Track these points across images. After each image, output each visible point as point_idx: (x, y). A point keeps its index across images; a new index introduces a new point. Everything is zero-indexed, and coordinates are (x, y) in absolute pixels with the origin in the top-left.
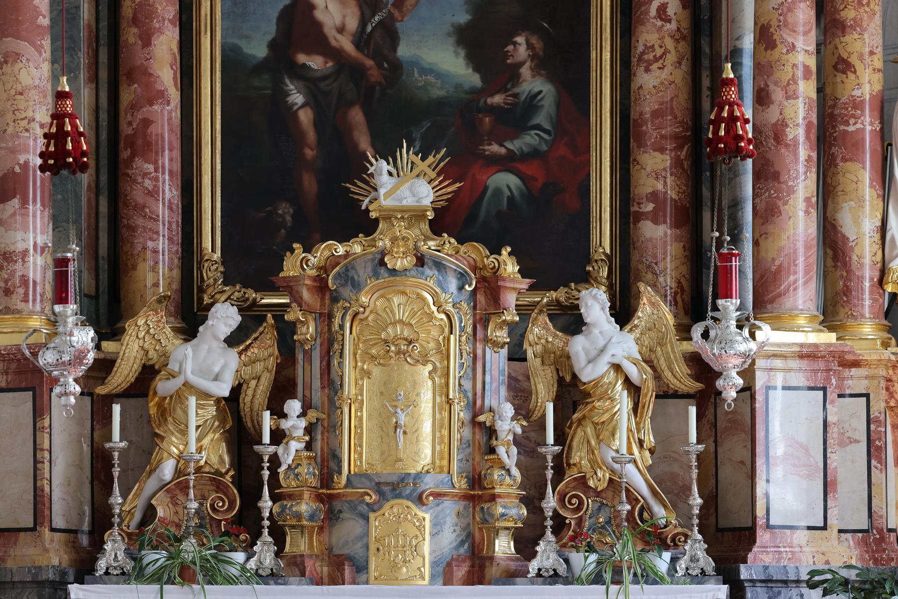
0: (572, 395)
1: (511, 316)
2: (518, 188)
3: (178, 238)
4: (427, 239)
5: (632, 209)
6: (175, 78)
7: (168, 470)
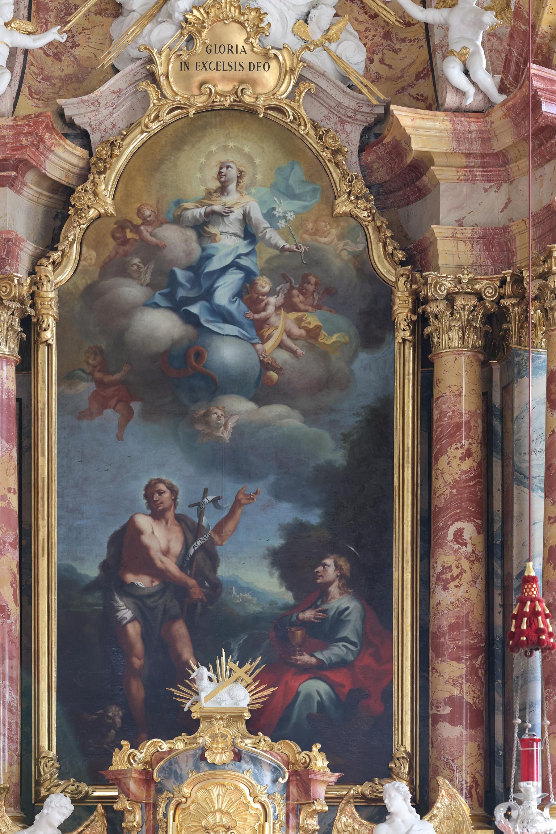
1: (321, 806)
2: (327, 693)
3: (18, 737)
4: (243, 737)
5: (431, 712)
6: (14, 595)
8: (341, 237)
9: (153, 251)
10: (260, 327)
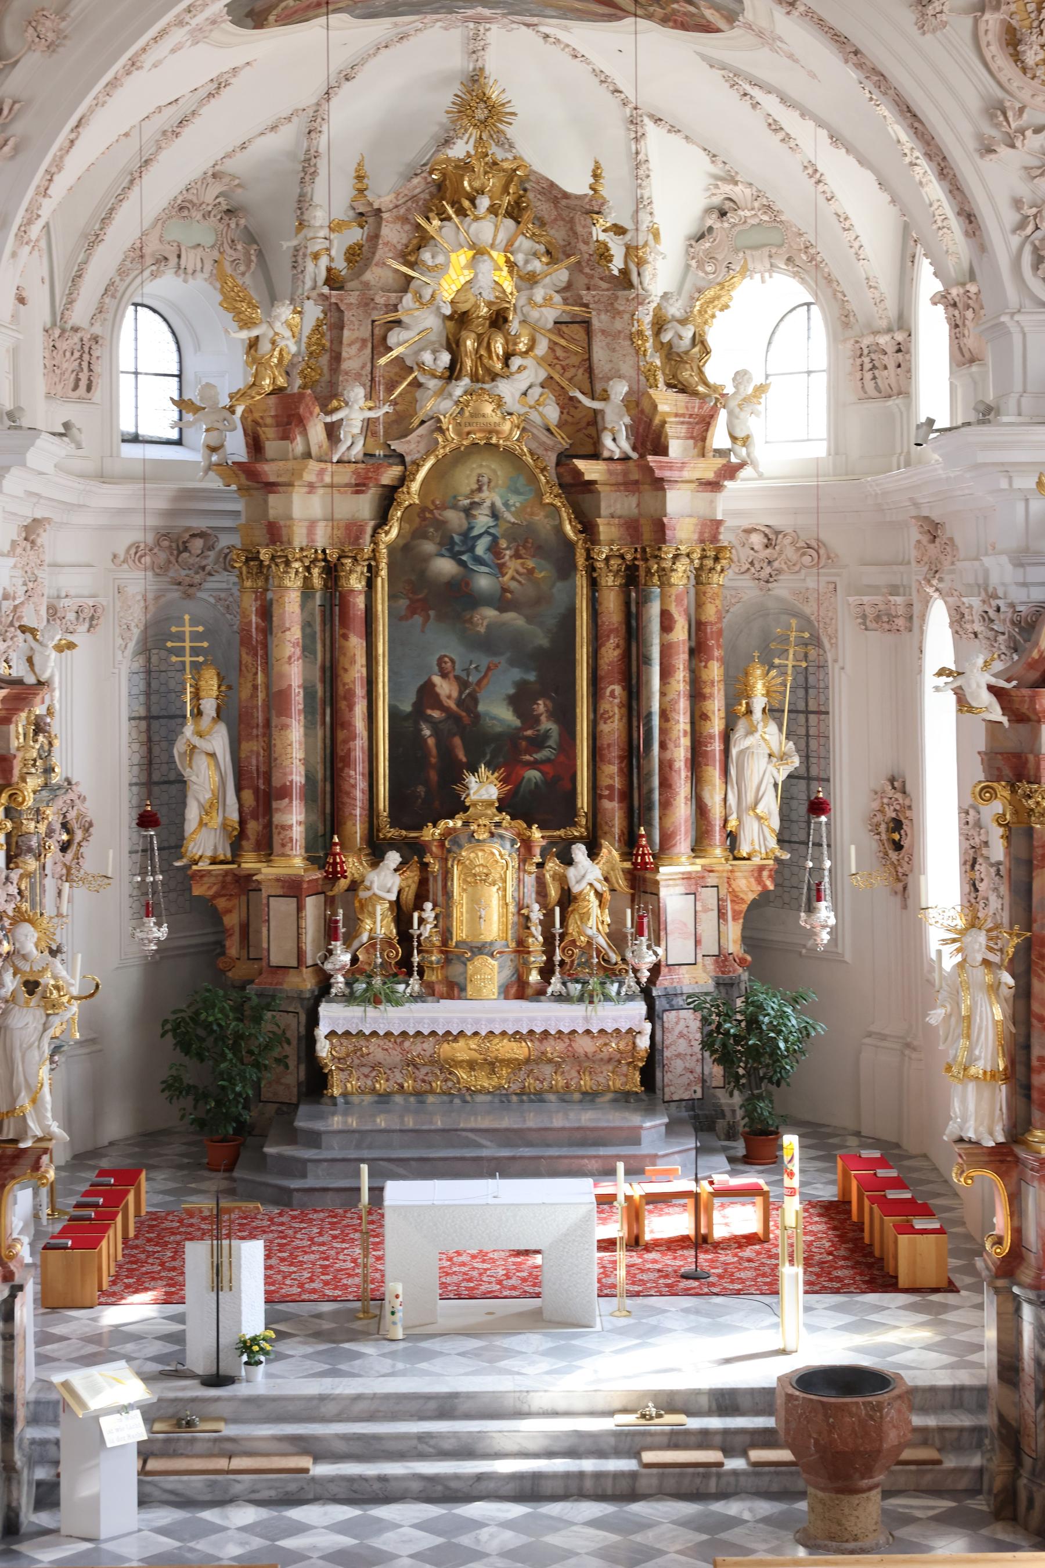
0: (568, 899)
7: (365, 937)
8: (546, 517)
9: (440, 524)
10: (501, 568)
